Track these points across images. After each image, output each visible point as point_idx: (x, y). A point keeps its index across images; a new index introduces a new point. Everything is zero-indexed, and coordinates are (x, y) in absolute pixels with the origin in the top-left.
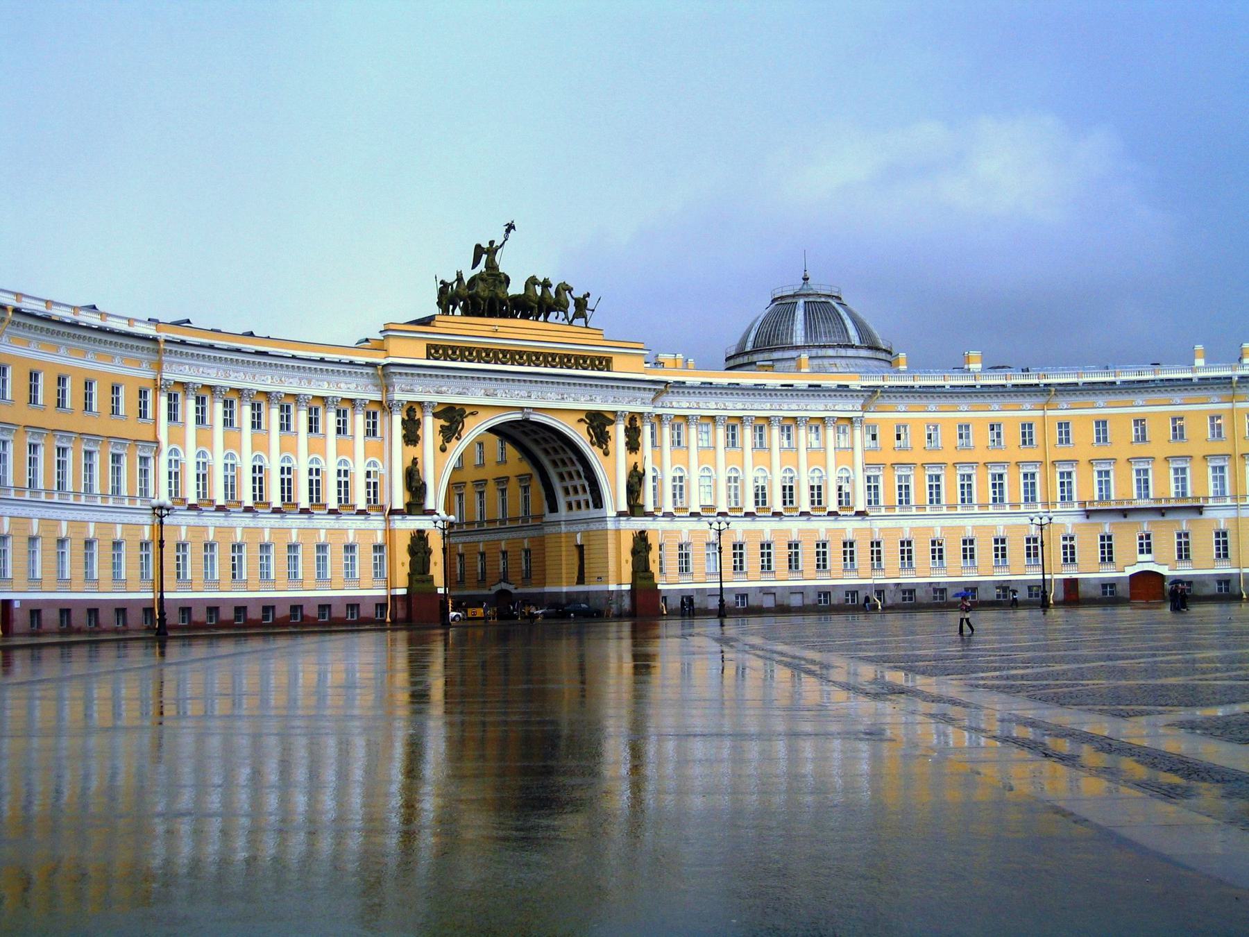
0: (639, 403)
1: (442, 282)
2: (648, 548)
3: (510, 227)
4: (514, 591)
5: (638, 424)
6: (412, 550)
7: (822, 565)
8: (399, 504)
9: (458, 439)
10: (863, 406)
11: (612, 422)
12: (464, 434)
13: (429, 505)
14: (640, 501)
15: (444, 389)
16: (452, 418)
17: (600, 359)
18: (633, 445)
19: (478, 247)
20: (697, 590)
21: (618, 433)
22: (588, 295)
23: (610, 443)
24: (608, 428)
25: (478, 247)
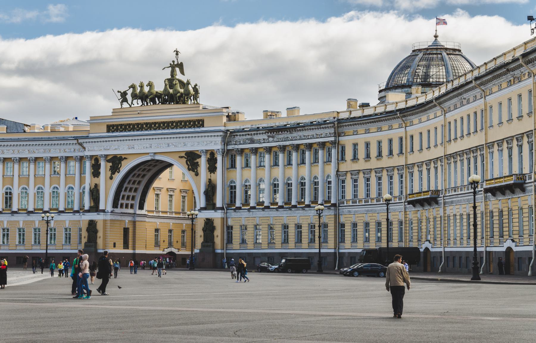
0: (212, 144)
1: (118, 92)
2: (213, 228)
3: (177, 53)
4: (177, 253)
5: (215, 156)
6: (88, 230)
7: (22, 241)
8: (87, 207)
9: (118, 172)
10: (335, 133)
11: (200, 157)
12: (121, 169)
13: (102, 207)
14: (214, 202)
15: (108, 148)
16: (116, 162)
17: (199, 121)
18: (212, 169)
19: (171, 64)
20: (248, 253)
21: (203, 162)
22: (196, 85)
23: (199, 169)
24: (198, 160)
25: (171, 64)
